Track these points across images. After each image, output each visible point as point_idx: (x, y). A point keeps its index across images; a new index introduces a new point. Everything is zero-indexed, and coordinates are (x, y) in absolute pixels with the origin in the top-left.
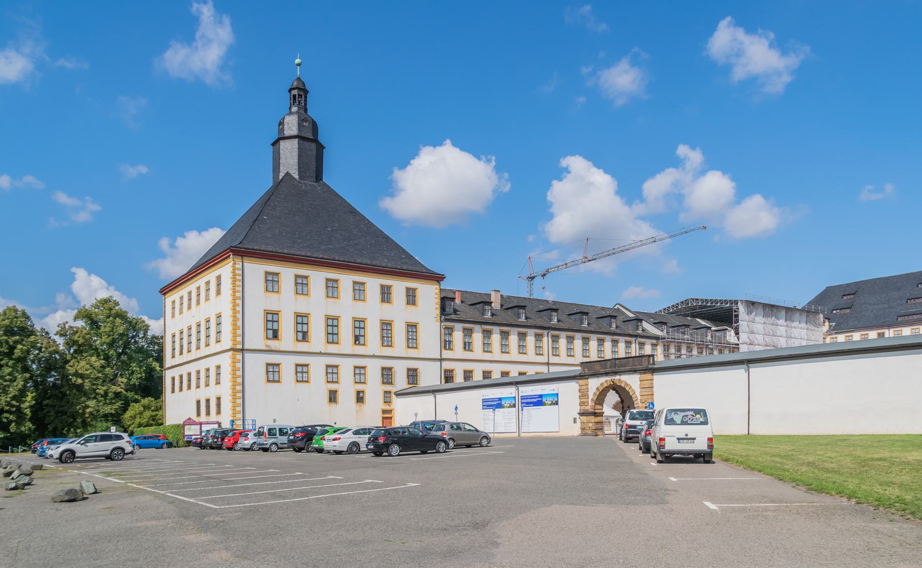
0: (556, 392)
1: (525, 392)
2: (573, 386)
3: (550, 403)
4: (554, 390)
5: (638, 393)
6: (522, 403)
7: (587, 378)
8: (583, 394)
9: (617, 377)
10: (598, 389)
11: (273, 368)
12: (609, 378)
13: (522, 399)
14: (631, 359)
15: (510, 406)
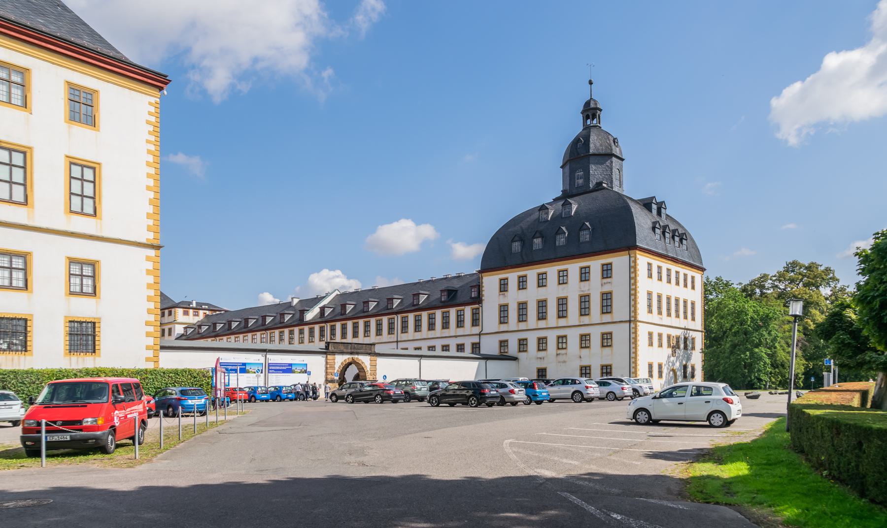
0: (305, 363)
1: (274, 360)
2: (320, 360)
3: (299, 371)
4: (303, 361)
5: (368, 369)
6: (269, 369)
7: (335, 355)
8: (328, 366)
9: (356, 356)
10: (342, 363)
11: (605, 339)
12: (350, 357)
13: (269, 366)
14: (364, 345)
15: (301, 372)
